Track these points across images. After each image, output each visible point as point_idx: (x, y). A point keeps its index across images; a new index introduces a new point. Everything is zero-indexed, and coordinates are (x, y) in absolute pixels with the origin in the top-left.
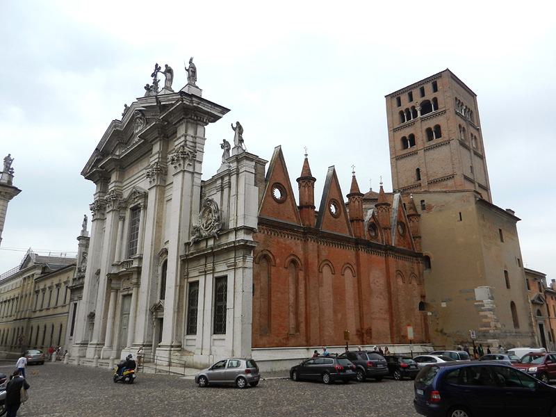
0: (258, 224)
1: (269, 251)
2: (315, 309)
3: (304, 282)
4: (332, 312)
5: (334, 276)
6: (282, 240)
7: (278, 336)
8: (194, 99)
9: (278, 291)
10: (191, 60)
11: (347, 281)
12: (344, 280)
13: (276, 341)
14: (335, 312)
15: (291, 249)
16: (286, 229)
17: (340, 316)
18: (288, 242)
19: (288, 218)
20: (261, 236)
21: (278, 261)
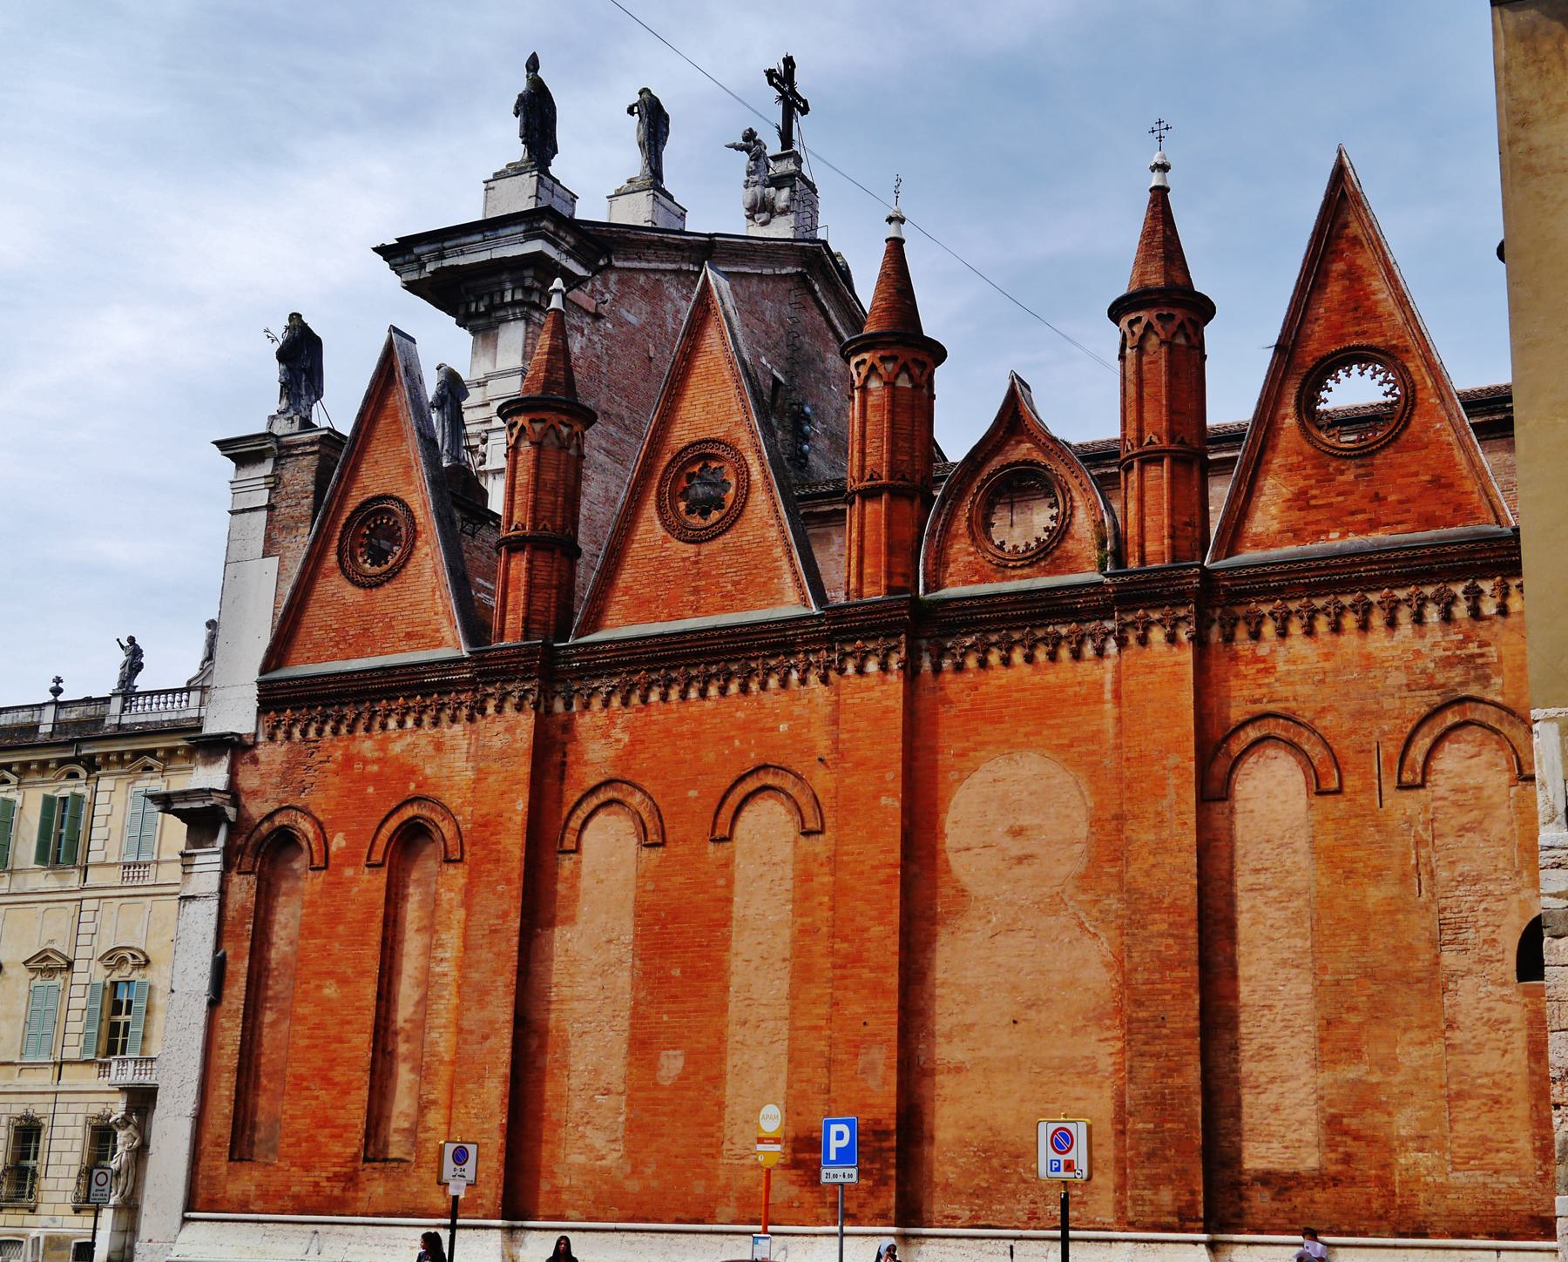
0: (262, 710)
1: (305, 811)
2: (485, 1038)
3: (460, 914)
4: (621, 1047)
5: (656, 855)
6: (366, 746)
7: (307, 1168)
8: (417, 250)
9: (330, 974)
10: (533, 64)
11: (744, 868)
12: (727, 864)
13: (295, 1189)
14: (642, 1046)
15: (412, 771)
16: (390, 694)
17: (672, 1064)
18: (397, 748)
19: (409, 636)
20: (272, 754)
21: (338, 842)
